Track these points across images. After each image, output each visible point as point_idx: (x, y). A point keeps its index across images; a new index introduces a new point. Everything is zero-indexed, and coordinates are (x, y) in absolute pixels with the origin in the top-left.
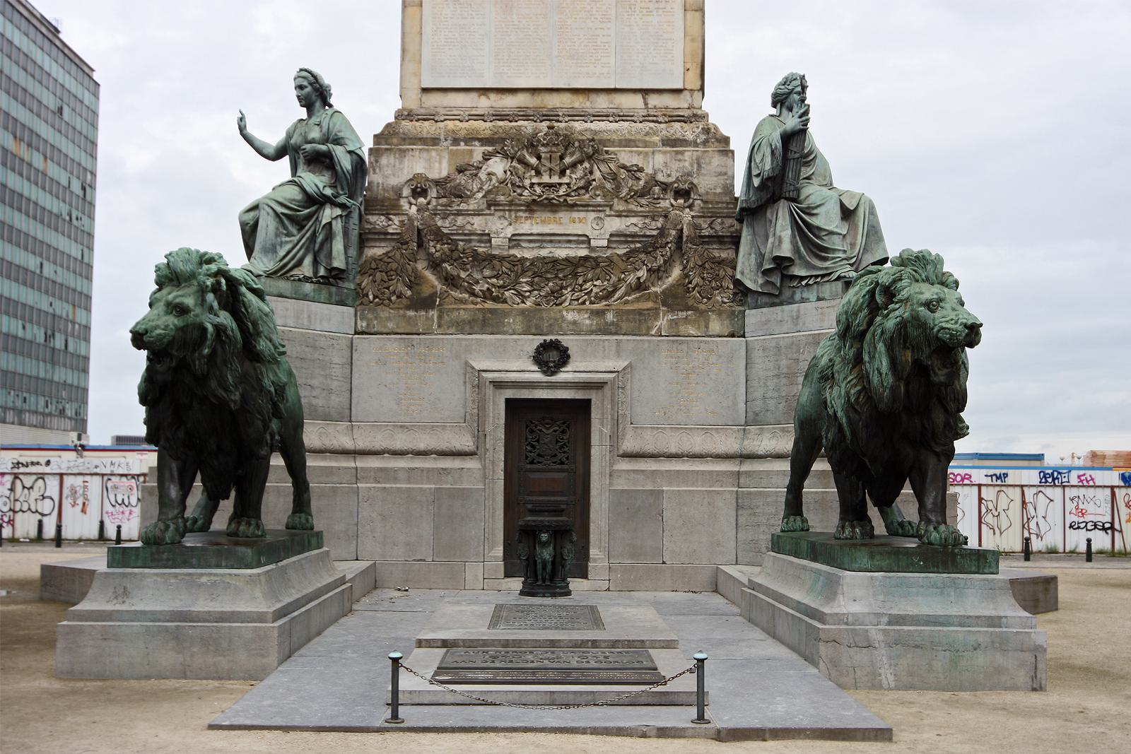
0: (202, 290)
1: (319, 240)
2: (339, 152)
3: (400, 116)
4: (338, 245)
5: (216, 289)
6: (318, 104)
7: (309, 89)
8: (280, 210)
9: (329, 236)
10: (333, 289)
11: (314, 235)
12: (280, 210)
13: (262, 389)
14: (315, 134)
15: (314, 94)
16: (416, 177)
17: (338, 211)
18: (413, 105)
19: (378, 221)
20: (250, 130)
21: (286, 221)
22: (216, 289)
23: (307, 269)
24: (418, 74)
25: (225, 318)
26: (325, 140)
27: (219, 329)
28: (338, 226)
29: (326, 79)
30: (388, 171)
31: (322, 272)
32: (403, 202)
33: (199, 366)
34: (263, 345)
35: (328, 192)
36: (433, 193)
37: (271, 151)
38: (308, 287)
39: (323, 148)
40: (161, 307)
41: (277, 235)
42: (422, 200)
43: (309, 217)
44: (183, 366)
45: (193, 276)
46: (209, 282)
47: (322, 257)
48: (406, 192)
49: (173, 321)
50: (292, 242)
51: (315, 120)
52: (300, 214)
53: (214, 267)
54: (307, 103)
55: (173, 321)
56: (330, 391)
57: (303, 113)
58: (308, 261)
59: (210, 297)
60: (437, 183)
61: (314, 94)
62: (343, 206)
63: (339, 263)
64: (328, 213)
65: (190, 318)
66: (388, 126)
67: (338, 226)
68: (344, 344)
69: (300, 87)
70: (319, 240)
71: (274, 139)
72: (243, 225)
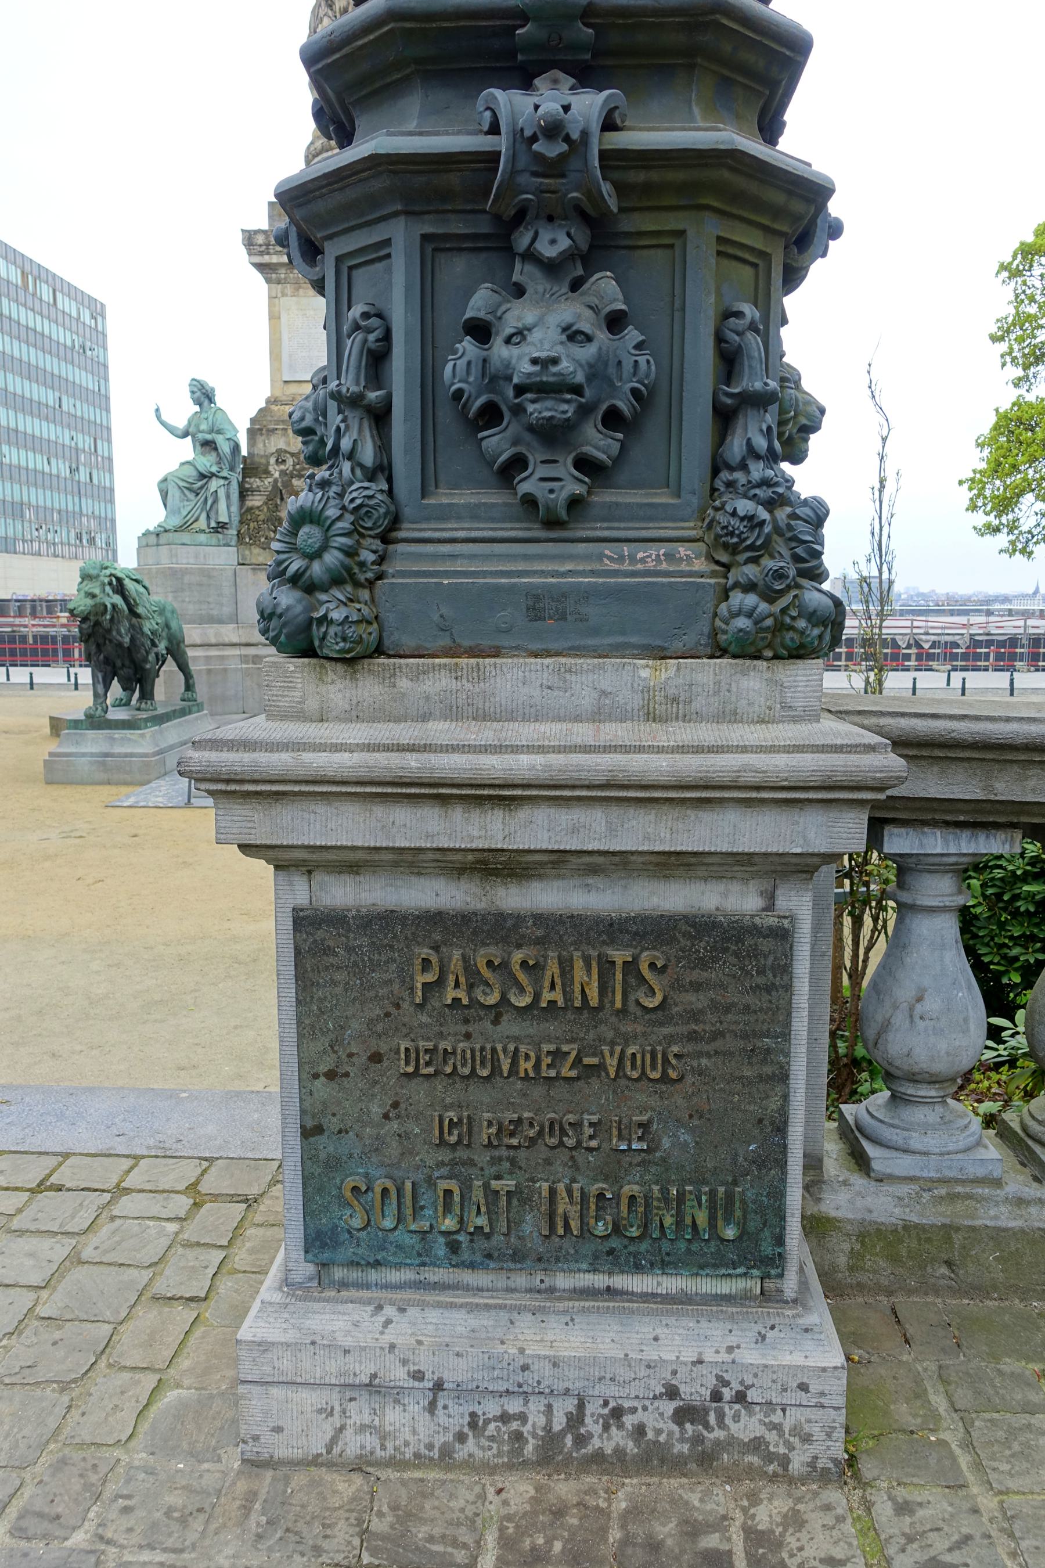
0: (103, 584)
1: (209, 503)
2: (220, 440)
3: (268, 401)
4: (222, 505)
5: (110, 584)
6: (206, 402)
7: (198, 394)
8: (182, 484)
9: (215, 501)
10: (220, 536)
11: (206, 499)
12: (182, 484)
13: (143, 633)
14: (204, 427)
15: (203, 395)
16: (279, 451)
17: (222, 482)
18: (278, 393)
19: (255, 482)
20: (164, 417)
21: (187, 492)
22: (110, 584)
23: (202, 523)
24: (280, 370)
25: (118, 600)
26: (211, 431)
27: (114, 606)
28: (222, 493)
29: (211, 382)
30: (261, 445)
31: (213, 524)
32: (271, 468)
33: (106, 624)
34: (140, 610)
35: (214, 469)
36: (290, 461)
37: (180, 433)
38: (202, 537)
39: (209, 437)
40: (82, 593)
41: (182, 501)
42: (282, 467)
43: (201, 488)
44: (97, 624)
45: (98, 576)
46: (106, 580)
47: (212, 515)
48: (272, 460)
49: (89, 602)
50: (190, 505)
51: (204, 415)
52: (196, 484)
53: (108, 572)
54: (198, 402)
55: (89, 602)
56: (222, 605)
57: (197, 408)
58: (204, 516)
59: (108, 589)
60: (292, 455)
61: (203, 395)
62: (225, 478)
63: (223, 518)
64: (214, 484)
65: (98, 600)
66: (261, 410)
67: (222, 493)
68: (230, 573)
69: (193, 392)
70: (209, 503)
71: (181, 424)
72: (161, 491)
